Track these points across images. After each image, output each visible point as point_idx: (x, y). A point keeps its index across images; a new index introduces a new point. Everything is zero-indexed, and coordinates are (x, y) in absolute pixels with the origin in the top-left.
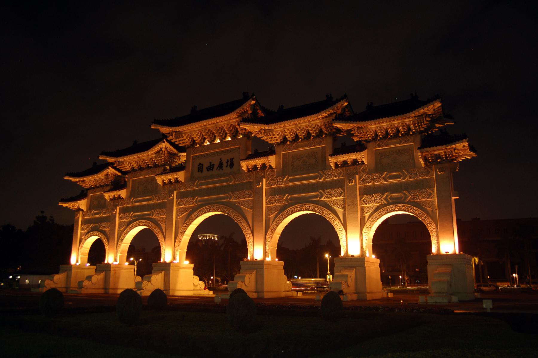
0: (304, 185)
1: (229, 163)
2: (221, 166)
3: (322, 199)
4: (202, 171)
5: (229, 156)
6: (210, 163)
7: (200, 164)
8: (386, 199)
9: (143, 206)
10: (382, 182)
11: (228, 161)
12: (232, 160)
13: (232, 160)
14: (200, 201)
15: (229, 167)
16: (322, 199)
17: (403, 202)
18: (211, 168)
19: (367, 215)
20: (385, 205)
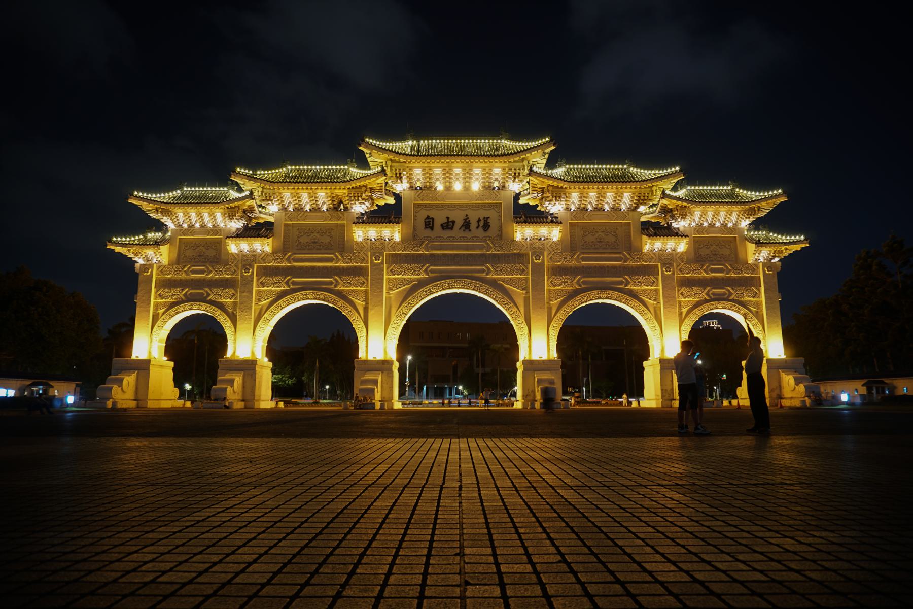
0: (602, 267)
1: (482, 224)
2: (467, 225)
3: (629, 287)
4: (432, 228)
5: (483, 214)
6: (448, 218)
7: (428, 217)
8: (707, 294)
9: (313, 268)
10: (703, 275)
11: (479, 220)
12: (486, 220)
13: (486, 220)
14: (432, 271)
15: (481, 229)
16: (629, 287)
17: (727, 300)
18: (448, 225)
19: (684, 311)
20: (706, 301)
